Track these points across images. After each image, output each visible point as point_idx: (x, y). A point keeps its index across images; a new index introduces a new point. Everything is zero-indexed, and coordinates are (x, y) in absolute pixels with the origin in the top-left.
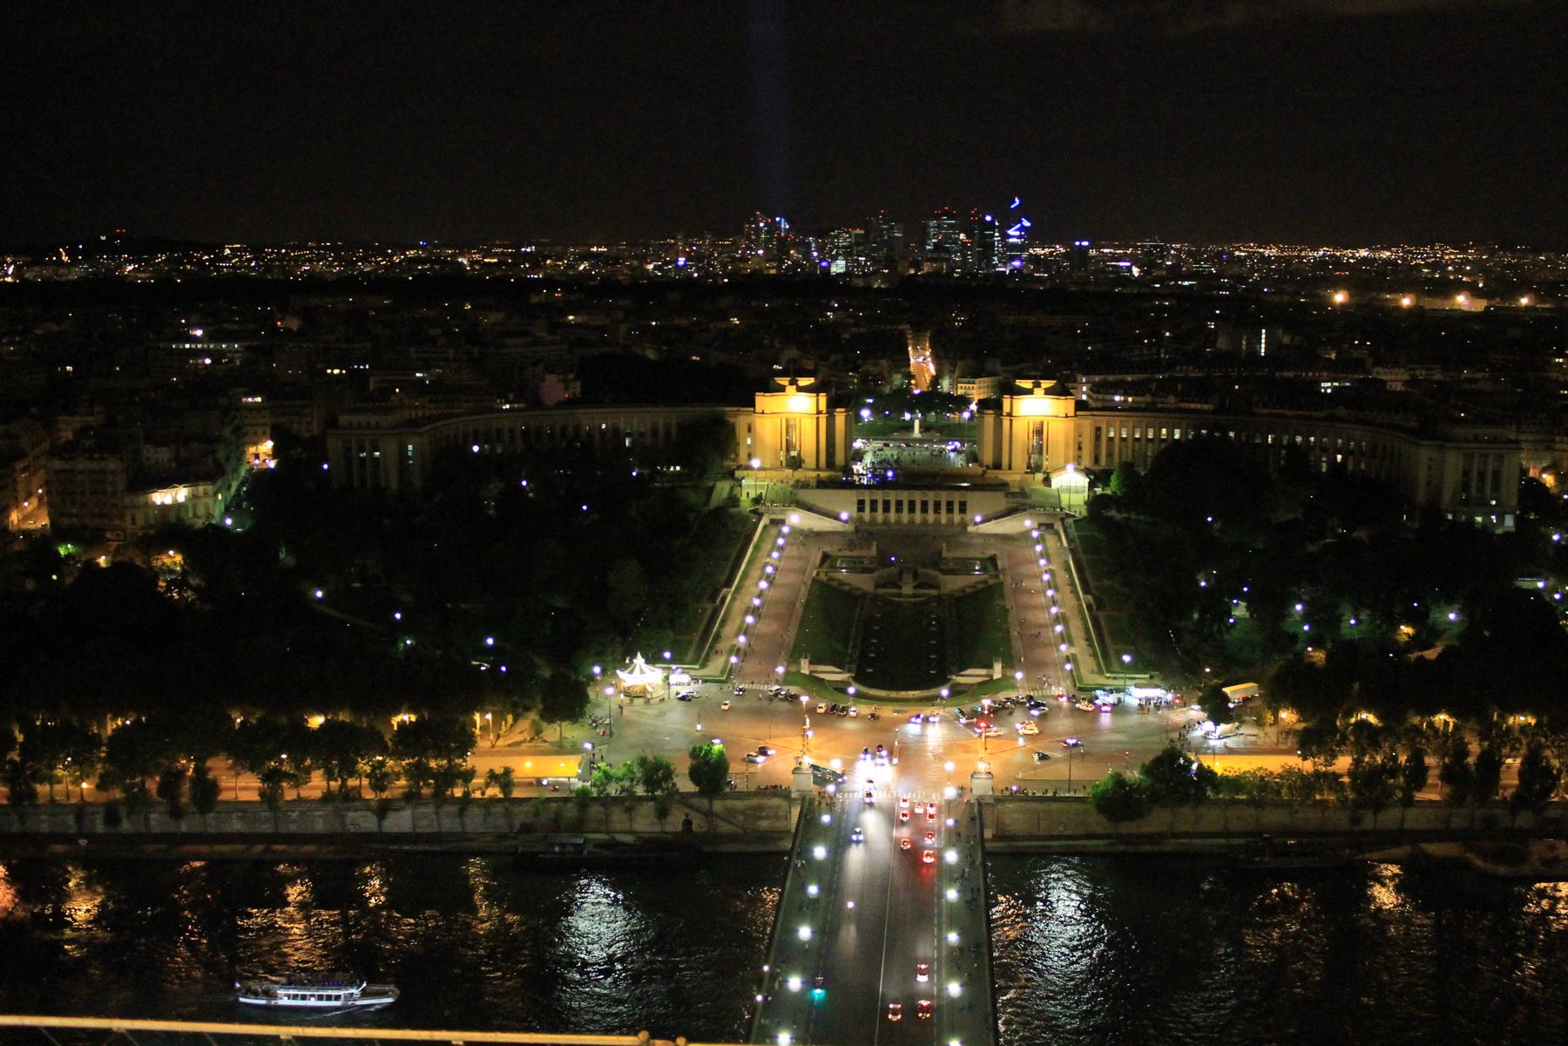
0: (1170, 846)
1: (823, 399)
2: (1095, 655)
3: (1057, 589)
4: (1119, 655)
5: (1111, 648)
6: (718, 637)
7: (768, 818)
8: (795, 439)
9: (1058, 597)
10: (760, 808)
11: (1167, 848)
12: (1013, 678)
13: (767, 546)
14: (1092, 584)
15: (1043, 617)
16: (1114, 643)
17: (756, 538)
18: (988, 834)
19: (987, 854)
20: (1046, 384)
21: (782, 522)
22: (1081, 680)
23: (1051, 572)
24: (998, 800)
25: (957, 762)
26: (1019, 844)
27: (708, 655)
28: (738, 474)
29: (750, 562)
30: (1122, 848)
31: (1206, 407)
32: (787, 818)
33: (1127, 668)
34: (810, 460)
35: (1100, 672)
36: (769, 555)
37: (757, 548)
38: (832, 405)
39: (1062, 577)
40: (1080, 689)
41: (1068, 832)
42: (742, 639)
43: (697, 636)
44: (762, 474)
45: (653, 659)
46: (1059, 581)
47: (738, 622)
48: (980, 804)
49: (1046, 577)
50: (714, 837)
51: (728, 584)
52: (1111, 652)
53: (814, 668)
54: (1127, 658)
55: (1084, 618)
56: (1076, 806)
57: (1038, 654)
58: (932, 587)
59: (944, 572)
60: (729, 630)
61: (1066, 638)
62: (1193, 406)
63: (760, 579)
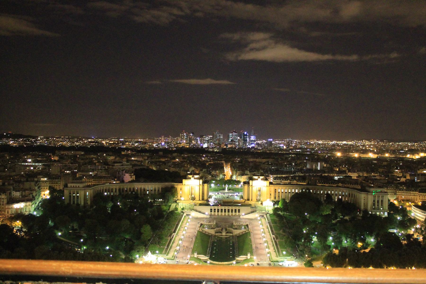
1: (201, 181)
2: (275, 251)
3: (265, 234)
4: (282, 251)
5: (280, 250)
6: (171, 247)
8: (193, 192)
9: (265, 236)
13: (185, 222)
15: (261, 241)
20: (262, 177)
21: (190, 215)
22: (272, 259)
23: (264, 229)
28: (178, 201)
31: (304, 184)
33: (284, 255)
34: (197, 198)
35: (277, 256)
36: (186, 224)
37: (183, 222)
38: (204, 182)
39: (266, 230)
40: (272, 261)
45: (153, 253)
47: (177, 243)
49: (262, 230)
51: (174, 232)
52: (280, 251)
53: (198, 255)
55: (272, 242)
57: (260, 252)
58: (231, 233)
60: (174, 245)
62: (301, 183)
63: (183, 230)
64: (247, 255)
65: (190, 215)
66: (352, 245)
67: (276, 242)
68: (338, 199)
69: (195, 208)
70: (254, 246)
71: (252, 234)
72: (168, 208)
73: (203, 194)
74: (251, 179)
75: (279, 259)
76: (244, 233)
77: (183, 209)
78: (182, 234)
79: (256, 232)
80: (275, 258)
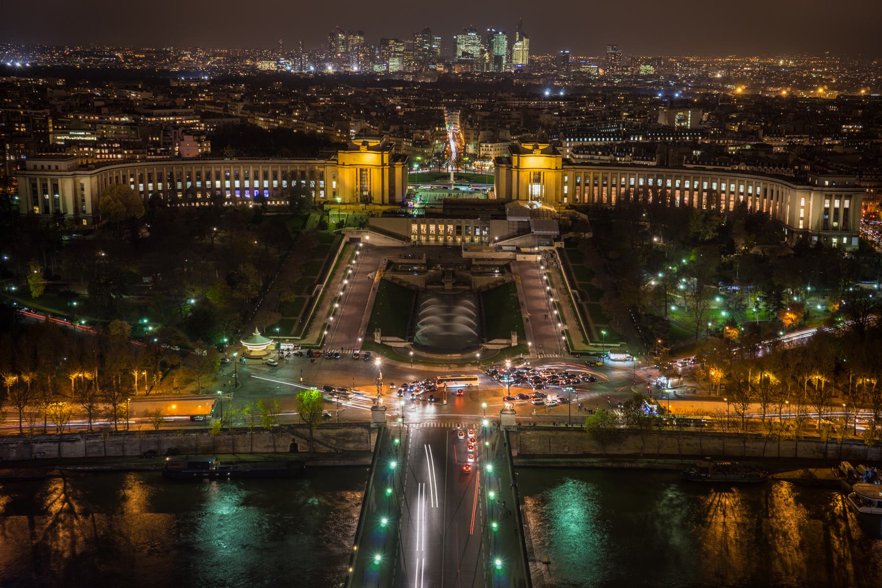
0: (642, 464)
1: (386, 156)
2: (581, 330)
3: (553, 287)
4: (598, 330)
5: (592, 326)
7: (353, 441)
8: (367, 185)
9: (554, 291)
10: (347, 434)
11: (641, 465)
12: (527, 346)
13: (348, 256)
14: (577, 283)
15: (543, 305)
17: (340, 251)
18: (515, 453)
19: (514, 467)
20: (542, 147)
21: (359, 240)
23: (549, 275)
24: (521, 428)
26: (538, 460)
28: (326, 207)
29: (336, 267)
30: (609, 464)
31: (651, 163)
32: (368, 441)
33: (602, 339)
34: (377, 198)
38: (394, 158)
39: (556, 278)
40: (572, 354)
41: (571, 453)
42: (331, 318)
43: (299, 319)
44: (344, 207)
46: (554, 280)
47: (328, 308)
48: (507, 432)
49: (545, 278)
51: (321, 281)
53: (384, 338)
56: (575, 434)
57: (543, 329)
58: (465, 284)
59: (473, 274)
61: (561, 319)
62: (642, 162)
63: (344, 278)
64: (509, 338)
66: (772, 317)
68: (737, 202)
69: (373, 222)
70: (527, 315)
71: (519, 288)
74: (517, 150)
75: (591, 348)
76: (499, 284)
77: (340, 225)
78: (340, 286)
79: (531, 282)
80: (579, 346)
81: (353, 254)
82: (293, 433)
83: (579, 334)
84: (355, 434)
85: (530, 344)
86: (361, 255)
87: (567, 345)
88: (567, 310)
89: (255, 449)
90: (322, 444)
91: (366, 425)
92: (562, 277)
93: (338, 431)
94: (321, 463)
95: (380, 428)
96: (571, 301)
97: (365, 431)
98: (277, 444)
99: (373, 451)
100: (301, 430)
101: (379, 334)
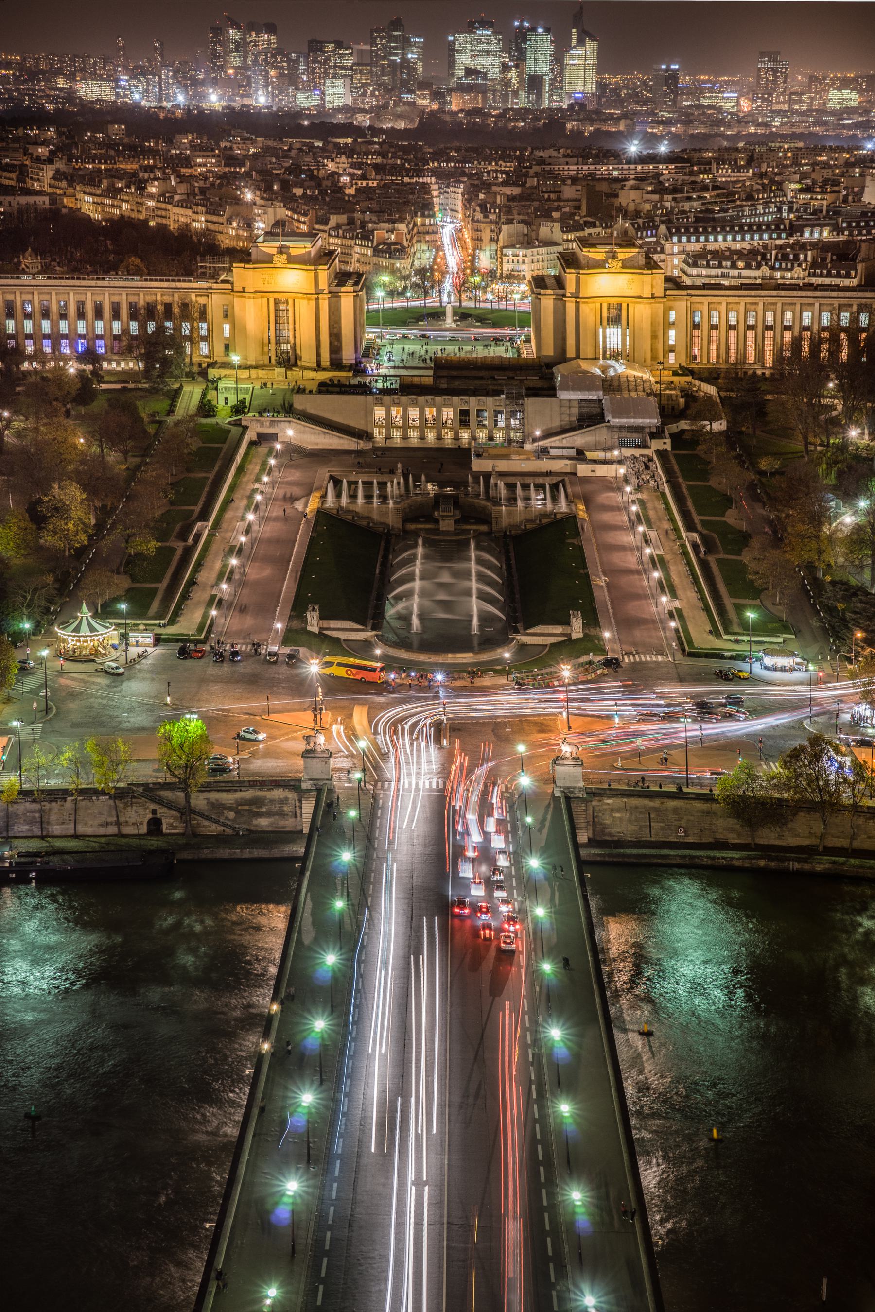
0: (822, 864)
1: (324, 275)
2: (707, 609)
4: (740, 609)
6: (192, 582)
7: (269, 814)
8: (288, 333)
9: (653, 535)
10: (257, 802)
11: (819, 868)
12: (600, 639)
13: (254, 468)
14: (697, 518)
15: (630, 561)
16: (733, 594)
17: (239, 458)
18: (583, 837)
19: (582, 864)
21: (273, 437)
22: (690, 642)
24: (593, 794)
25: (533, 745)
26: (628, 851)
27: (178, 608)
28: (213, 373)
29: (232, 489)
30: (762, 863)
33: (746, 628)
34: (308, 357)
35: (715, 632)
36: (258, 480)
37: (241, 470)
38: (342, 278)
40: (691, 655)
42: (224, 586)
44: (244, 374)
47: (218, 565)
50: (194, 838)
51: (204, 516)
52: (729, 608)
53: (325, 624)
54: (751, 615)
55: (689, 563)
57: (632, 608)
60: (206, 576)
61: (668, 587)
63: (247, 508)
64: (568, 623)
65: (273, 437)
67: (704, 565)
69: (300, 402)
70: (600, 581)
72: (165, 405)
73: (335, 336)
75: (724, 644)
77: (239, 409)
78: (241, 526)
79: (607, 517)
80: (703, 639)
81: (264, 464)
82: (153, 800)
83: (703, 615)
84: (272, 801)
85: (607, 635)
86: (279, 466)
87: (679, 638)
88: (678, 571)
89: (81, 829)
90: (208, 818)
91: (293, 785)
92: (668, 508)
93: (239, 795)
94: (206, 853)
95: (319, 791)
96: (685, 554)
97: (291, 795)
98: (122, 819)
99: (306, 831)
100: (167, 794)
101: (316, 615)
